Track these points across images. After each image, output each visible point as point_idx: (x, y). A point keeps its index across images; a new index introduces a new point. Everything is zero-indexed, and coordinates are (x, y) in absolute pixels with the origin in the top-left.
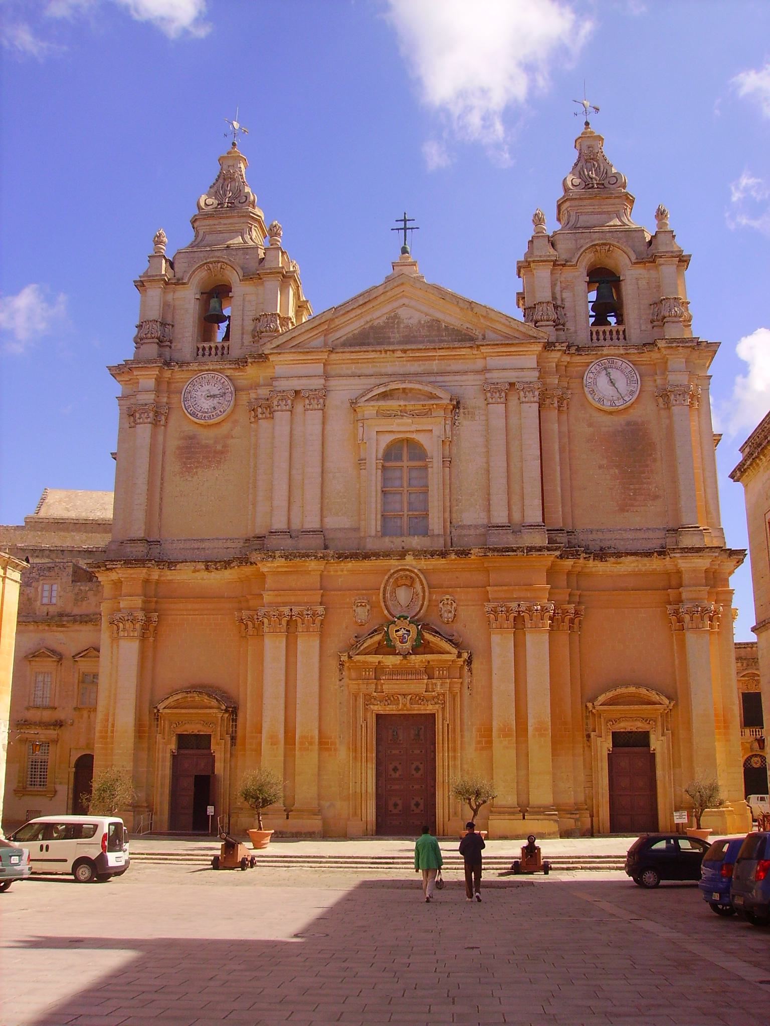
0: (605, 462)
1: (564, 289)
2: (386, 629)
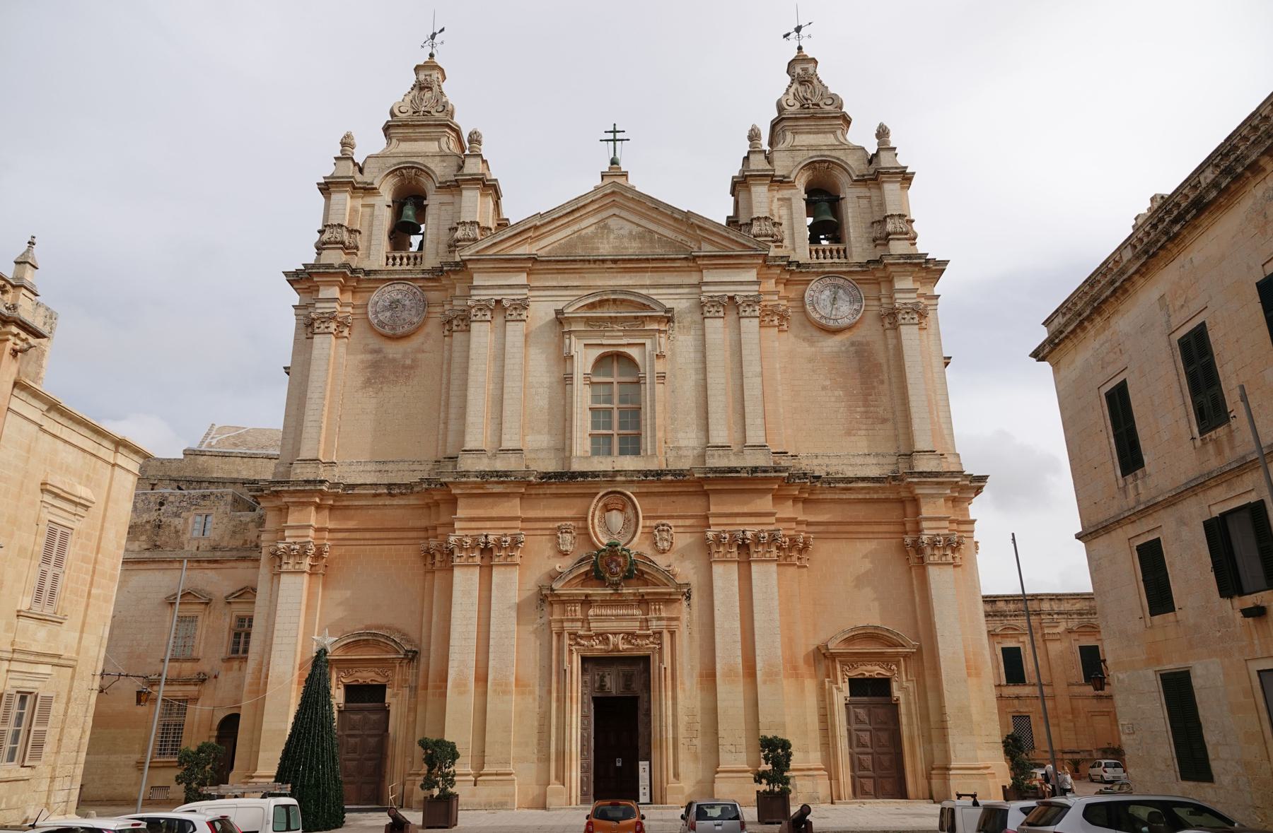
0: (828, 383)
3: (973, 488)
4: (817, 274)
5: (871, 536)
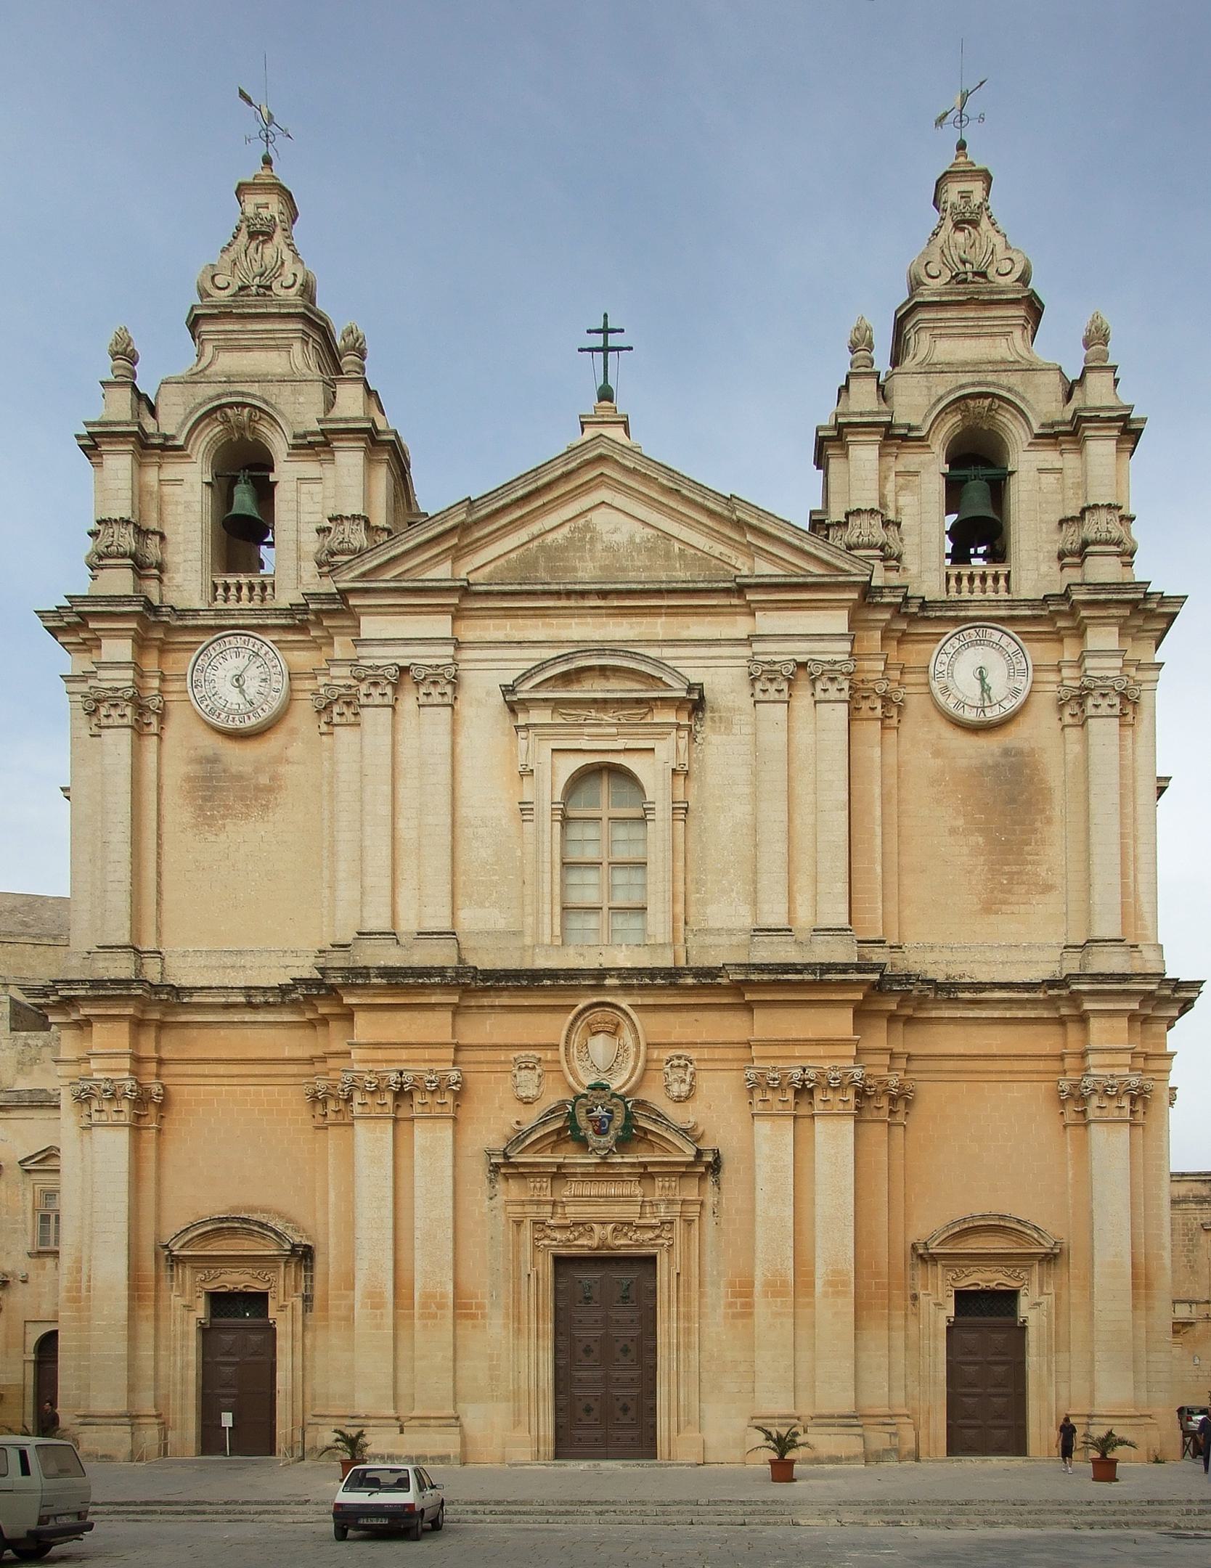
1: (901, 489)
2: (570, 1107)
3: (1178, 1000)
4: (956, 621)
5: (1008, 1077)
